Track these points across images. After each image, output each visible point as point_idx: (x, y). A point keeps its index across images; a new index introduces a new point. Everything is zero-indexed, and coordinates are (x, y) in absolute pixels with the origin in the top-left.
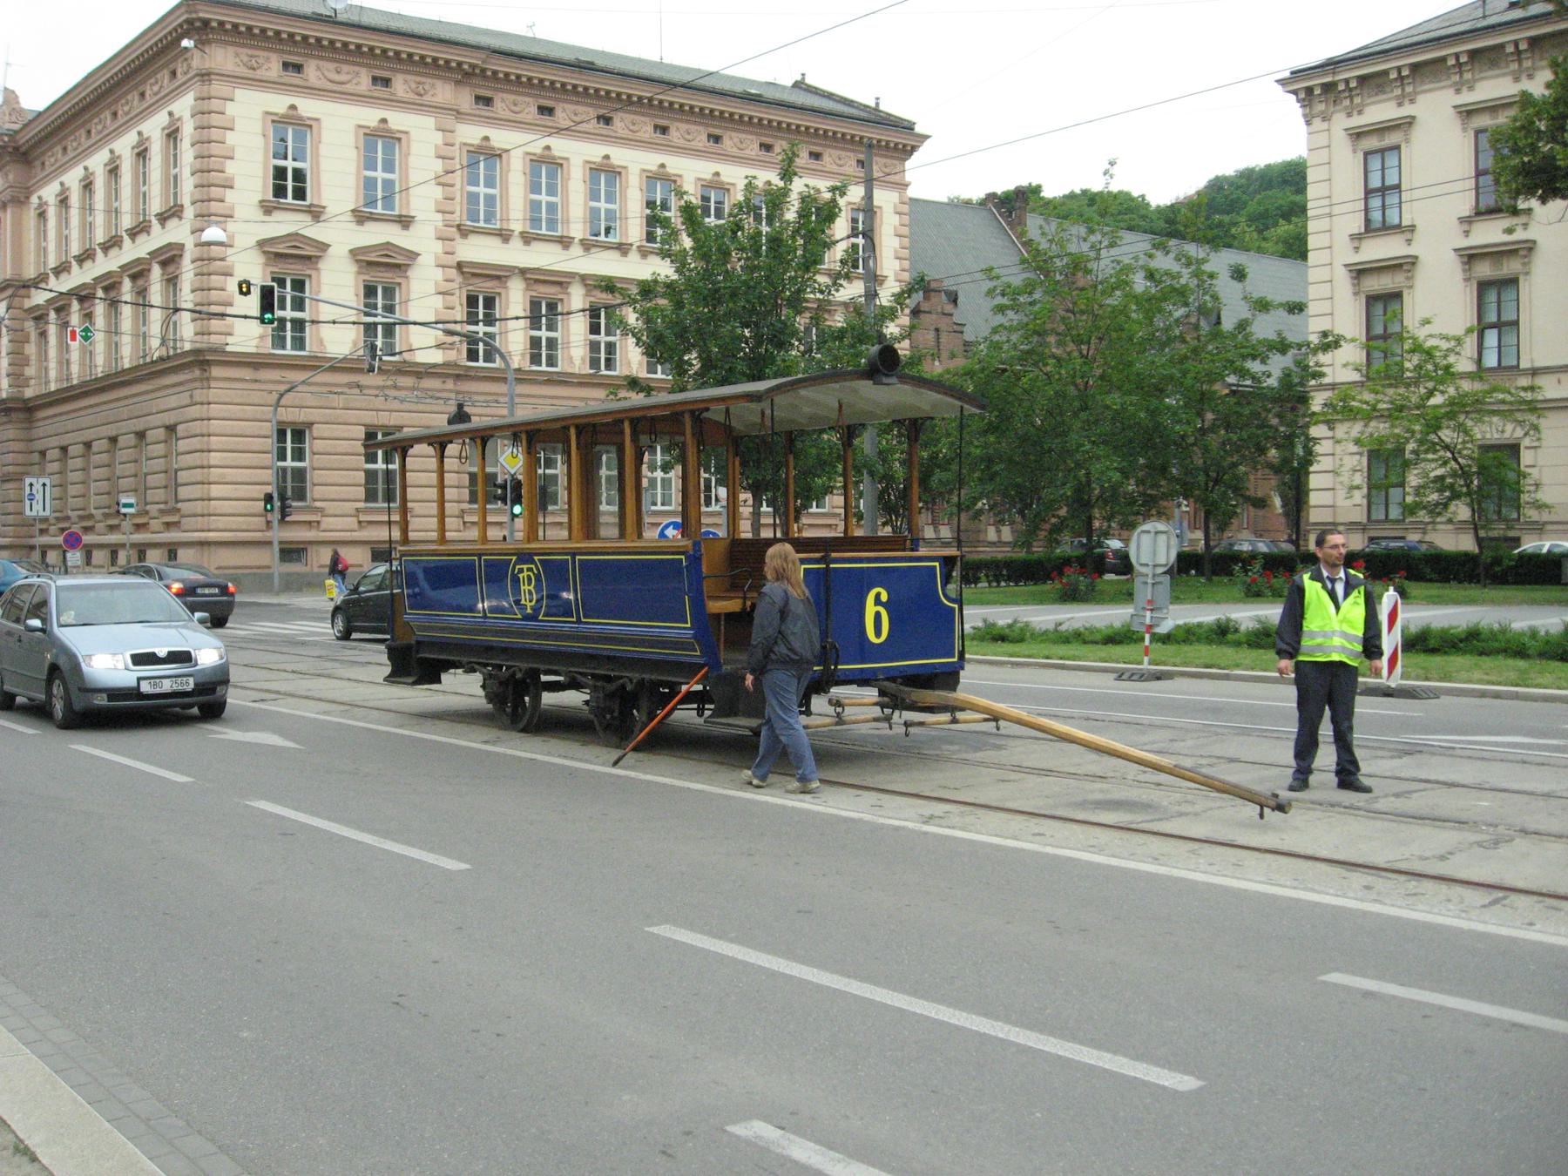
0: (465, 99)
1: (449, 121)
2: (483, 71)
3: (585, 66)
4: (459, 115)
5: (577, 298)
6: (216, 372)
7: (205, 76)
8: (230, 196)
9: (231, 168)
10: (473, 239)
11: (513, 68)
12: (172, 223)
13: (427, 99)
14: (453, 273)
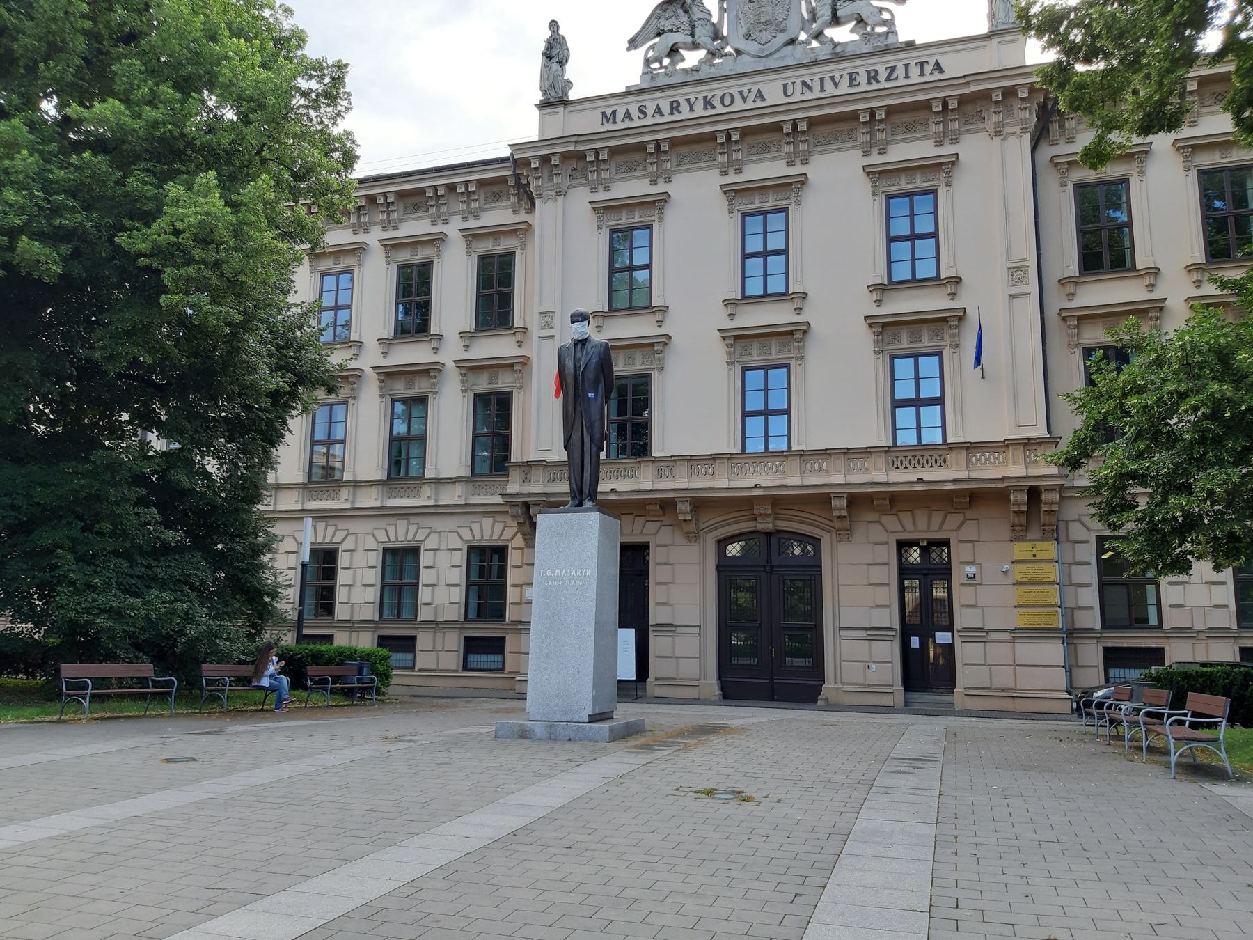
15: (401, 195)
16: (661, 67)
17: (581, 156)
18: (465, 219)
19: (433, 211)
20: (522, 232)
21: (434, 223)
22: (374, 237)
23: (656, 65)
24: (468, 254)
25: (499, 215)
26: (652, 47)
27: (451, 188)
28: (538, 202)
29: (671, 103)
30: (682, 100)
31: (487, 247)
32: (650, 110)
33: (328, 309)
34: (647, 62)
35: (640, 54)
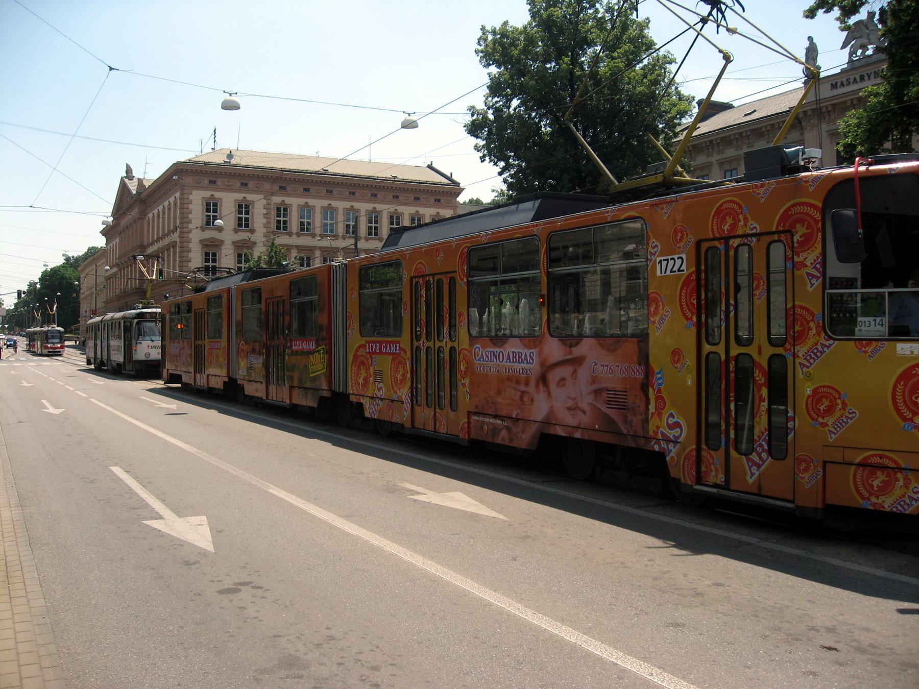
0: (276, 187)
9: (190, 216)
12: (175, 233)
16: (856, 56)
23: (854, 55)
28: (806, 132)
29: (860, 76)
30: (865, 74)
32: (852, 80)
34: (851, 55)
35: (847, 50)
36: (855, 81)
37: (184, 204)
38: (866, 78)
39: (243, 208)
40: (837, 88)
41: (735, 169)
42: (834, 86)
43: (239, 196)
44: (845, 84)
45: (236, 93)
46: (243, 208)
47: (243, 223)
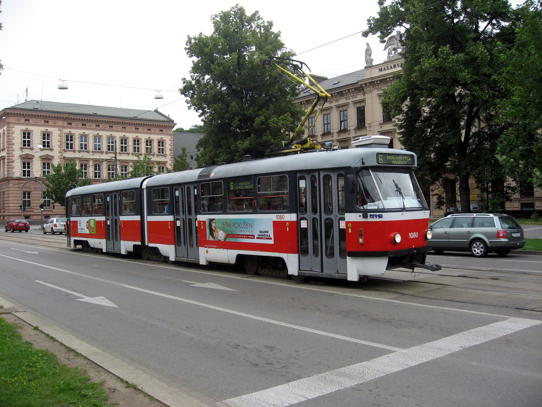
0: (65, 124)
1: (61, 129)
2: (69, 118)
3: (95, 115)
4: (64, 127)
5: (91, 163)
6: (11, 181)
7: (8, 123)
8: (14, 147)
10: (67, 152)
11: (75, 117)
12: (4, 151)
13: (57, 125)
14: (62, 160)
15: (338, 93)
16: (392, 54)
17: (374, 82)
18: (353, 98)
19: (346, 96)
20: (364, 101)
21: (346, 100)
22: (334, 104)
23: (390, 54)
24: (354, 107)
25: (360, 97)
26: (389, 49)
27: (349, 90)
28: (366, 95)
29: (394, 65)
30: (396, 64)
31: (359, 105)
32: (389, 67)
33: (326, 124)
34: (389, 54)
35: (387, 50)
36: (391, 67)
37: (9, 133)
38: (397, 66)
39: (46, 136)
40: (382, 71)
41: (329, 114)
42: (381, 70)
43: (44, 129)
44: (386, 69)
45: (66, 80)
46: (46, 136)
47: (46, 145)
